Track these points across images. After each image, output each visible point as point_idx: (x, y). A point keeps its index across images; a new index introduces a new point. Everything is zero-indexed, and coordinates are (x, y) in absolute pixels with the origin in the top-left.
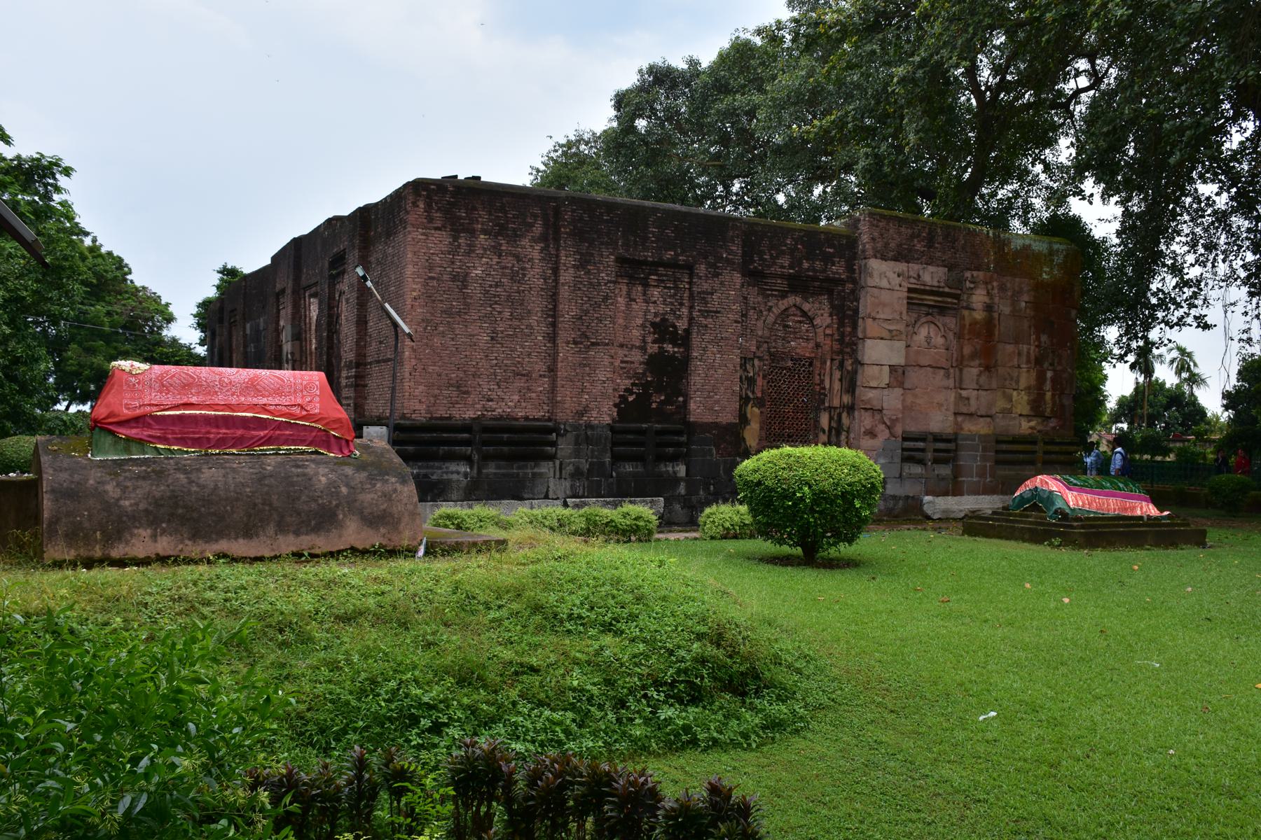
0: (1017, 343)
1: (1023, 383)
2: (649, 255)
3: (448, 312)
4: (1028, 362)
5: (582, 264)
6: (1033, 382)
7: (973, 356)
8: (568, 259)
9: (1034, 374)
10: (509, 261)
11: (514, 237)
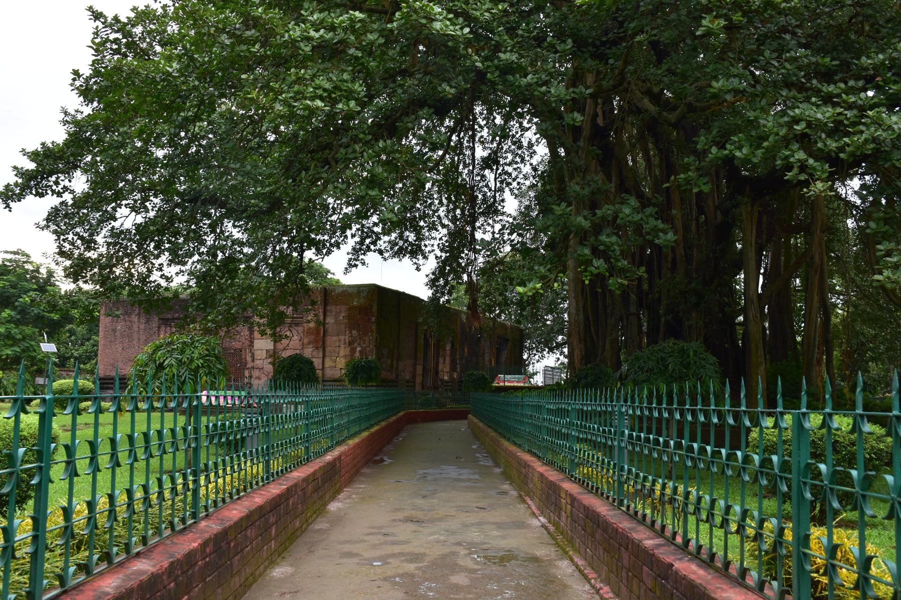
0: (338, 335)
1: (342, 354)
2: (169, 316)
3: (110, 342)
4: (345, 344)
5: (147, 322)
6: (348, 353)
7: (309, 343)
8: (143, 321)
9: (348, 349)
10: (128, 323)
11: (130, 315)
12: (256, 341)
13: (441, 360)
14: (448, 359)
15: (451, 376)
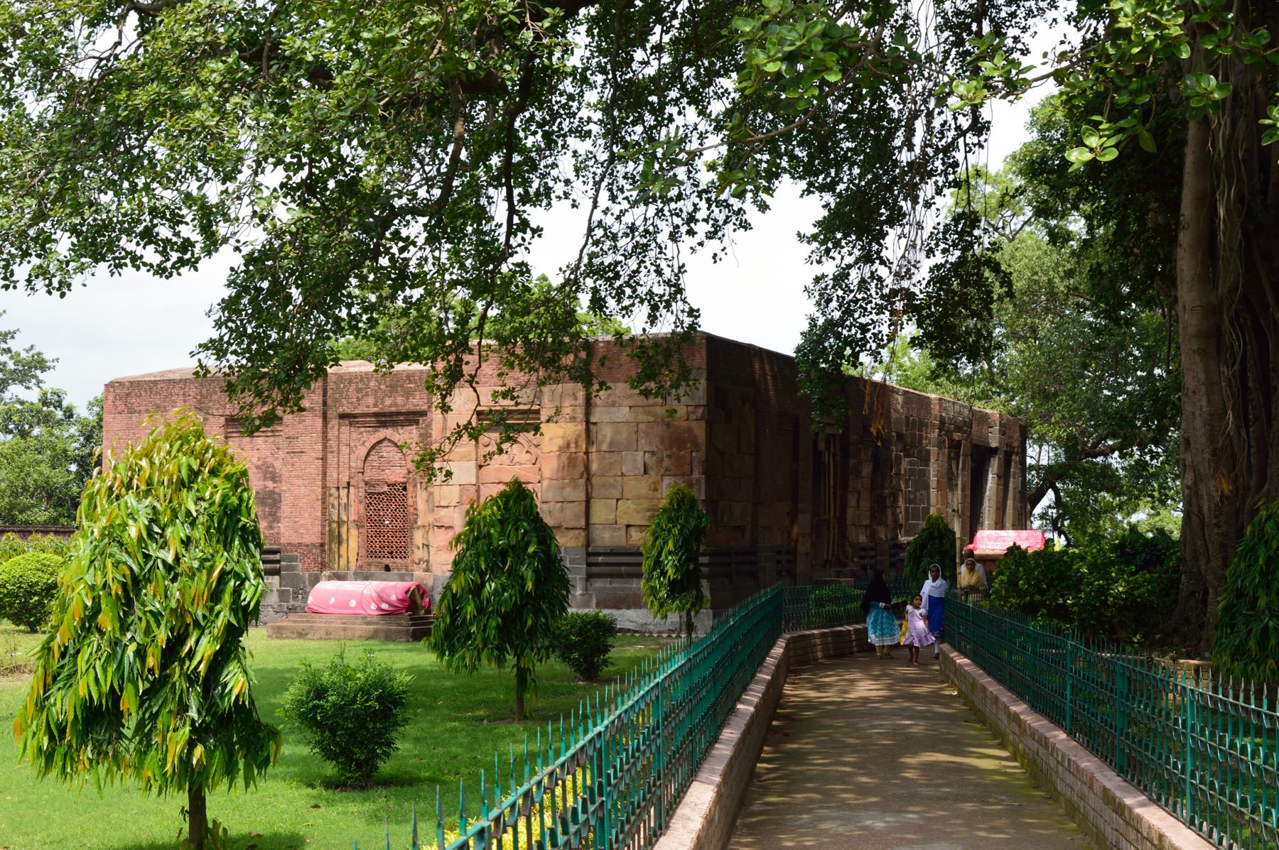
13: (852, 500)
14: (866, 496)
15: (873, 535)
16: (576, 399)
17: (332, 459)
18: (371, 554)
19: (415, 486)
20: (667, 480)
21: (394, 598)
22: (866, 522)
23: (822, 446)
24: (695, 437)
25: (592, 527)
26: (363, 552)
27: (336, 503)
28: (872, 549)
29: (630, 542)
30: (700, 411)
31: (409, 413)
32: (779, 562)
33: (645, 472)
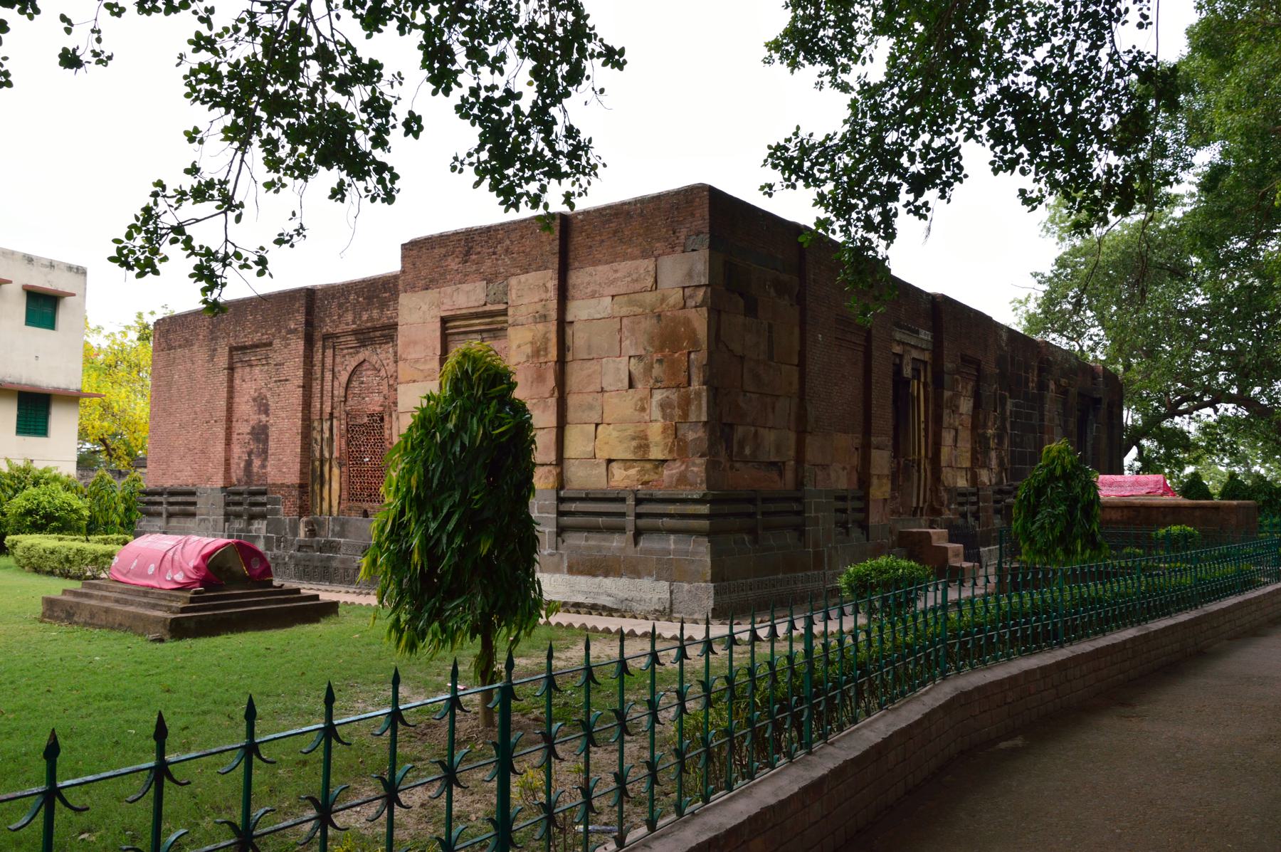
12: (401, 388)
13: (948, 437)
14: (965, 435)
15: (974, 479)
16: (547, 291)
17: (316, 387)
18: (353, 497)
19: (391, 415)
20: (658, 396)
21: (192, 564)
22: (967, 464)
23: (907, 372)
24: (694, 331)
25: (566, 463)
26: (345, 496)
27: (319, 438)
28: (973, 494)
29: (612, 484)
30: (701, 293)
31: (384, 327)
32: (844, 511)
33: (631, 385)
